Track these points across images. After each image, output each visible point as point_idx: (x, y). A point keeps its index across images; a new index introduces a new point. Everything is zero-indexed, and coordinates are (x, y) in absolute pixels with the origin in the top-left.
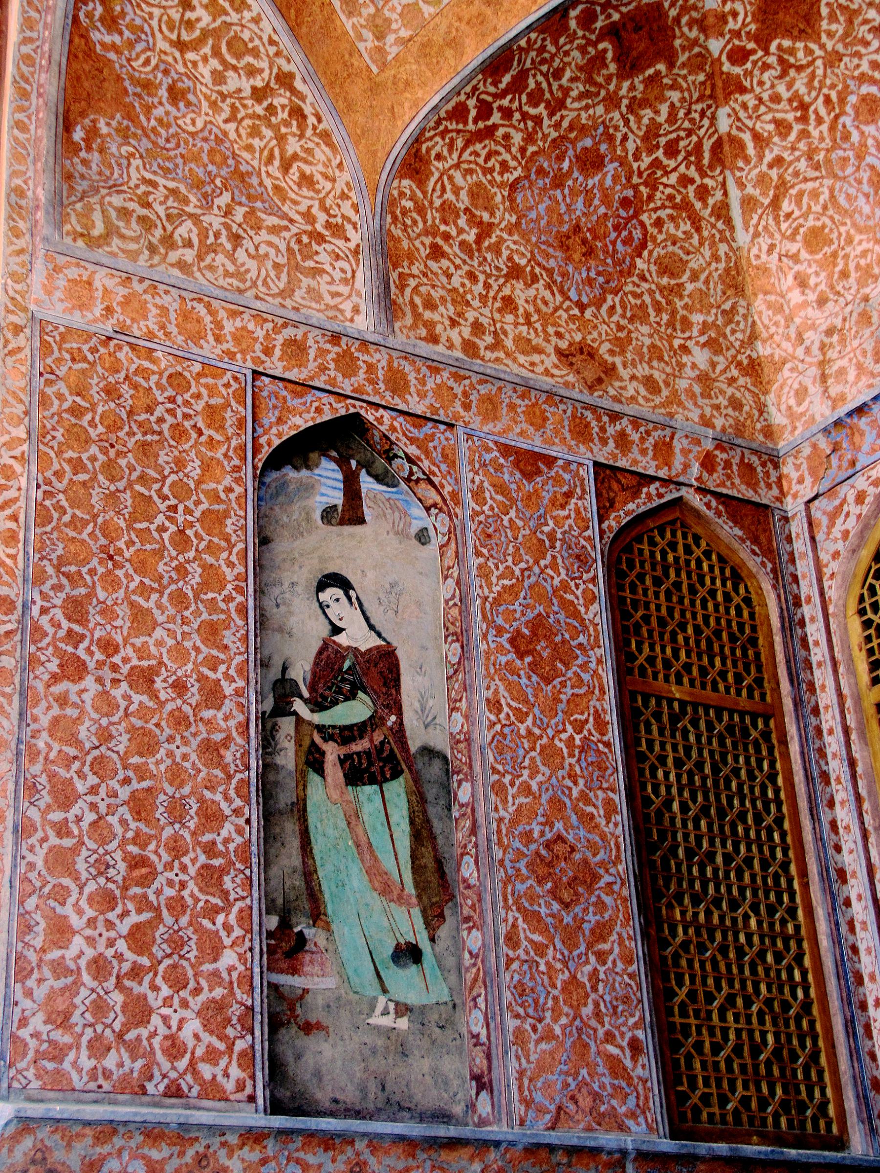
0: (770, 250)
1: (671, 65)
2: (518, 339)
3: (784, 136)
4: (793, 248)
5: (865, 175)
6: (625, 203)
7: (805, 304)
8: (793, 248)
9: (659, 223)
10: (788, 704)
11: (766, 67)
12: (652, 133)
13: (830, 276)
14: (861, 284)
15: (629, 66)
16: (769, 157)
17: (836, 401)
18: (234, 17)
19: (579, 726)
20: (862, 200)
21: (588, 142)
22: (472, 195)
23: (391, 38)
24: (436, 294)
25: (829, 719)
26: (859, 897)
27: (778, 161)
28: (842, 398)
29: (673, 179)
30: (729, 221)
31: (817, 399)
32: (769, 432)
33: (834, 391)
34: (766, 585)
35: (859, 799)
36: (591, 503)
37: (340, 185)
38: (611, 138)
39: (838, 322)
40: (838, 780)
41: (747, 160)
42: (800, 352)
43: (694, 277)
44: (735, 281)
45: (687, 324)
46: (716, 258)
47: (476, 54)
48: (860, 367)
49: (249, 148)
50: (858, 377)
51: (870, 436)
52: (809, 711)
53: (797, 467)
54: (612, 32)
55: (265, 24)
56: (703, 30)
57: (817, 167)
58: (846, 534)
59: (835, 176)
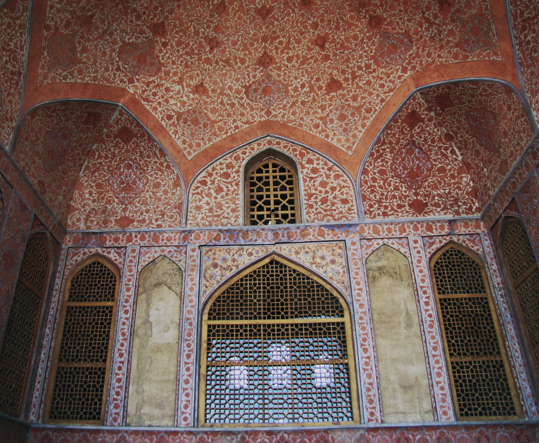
0: (86, 182)
1: (94, 128)
2: (33, 172)
3: (106, 159)
4: (93, 184)
5: (119, 180)
6: (65, 151)
7: (89, 199)
8: (93, 184)
9: (68, 160)
10: (46, 297)
11: (112, 142)
12: (80, 139)
13: (99, 197)
14: (106, 203)
15: (87, 122)
16: (99, 161)
17: (88, 227)
18: (19, 51)
19: (9, 285)
20: (115, 185)
21: (67, 132)
22: (39, 129)
23: (46, 81)
24: (23, 150)
25: (53, 305)
26: (44, 354)
27: (101, 163)
28: (90, 227)
29: (76, 152)
30: (81, 169)
31: (83, 224)
32: (66, 224)
33: (89, 224)
34: (52, 264)
35: (54, 329)
36: (30, 224)
37: (17, 108)
38: (71, 135)
39: (97, 208)
40: (50, 322)
41: (94, 158)
42: (83, 210)
43: (67, 178)
44: (75, 183)
45: (61, 189)
46: (73, 175)
47: (62, 97)
48: (98, 223)
49: (3, 85)
50: (96, 225)
51: (94, 241)
52: (49, 301)
53: (70, 237)
54: (89, 113)
55: (24, 58)
56: (105, 126)
57: (109, 170)
58: (76, 261)
59: (112, 176)
